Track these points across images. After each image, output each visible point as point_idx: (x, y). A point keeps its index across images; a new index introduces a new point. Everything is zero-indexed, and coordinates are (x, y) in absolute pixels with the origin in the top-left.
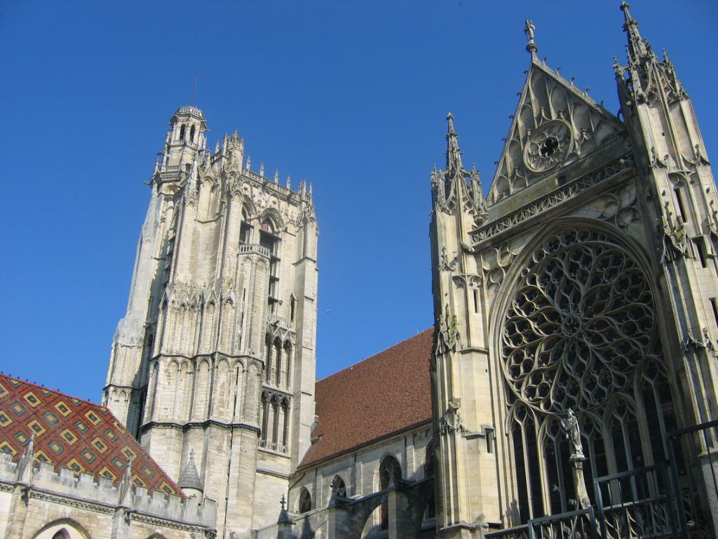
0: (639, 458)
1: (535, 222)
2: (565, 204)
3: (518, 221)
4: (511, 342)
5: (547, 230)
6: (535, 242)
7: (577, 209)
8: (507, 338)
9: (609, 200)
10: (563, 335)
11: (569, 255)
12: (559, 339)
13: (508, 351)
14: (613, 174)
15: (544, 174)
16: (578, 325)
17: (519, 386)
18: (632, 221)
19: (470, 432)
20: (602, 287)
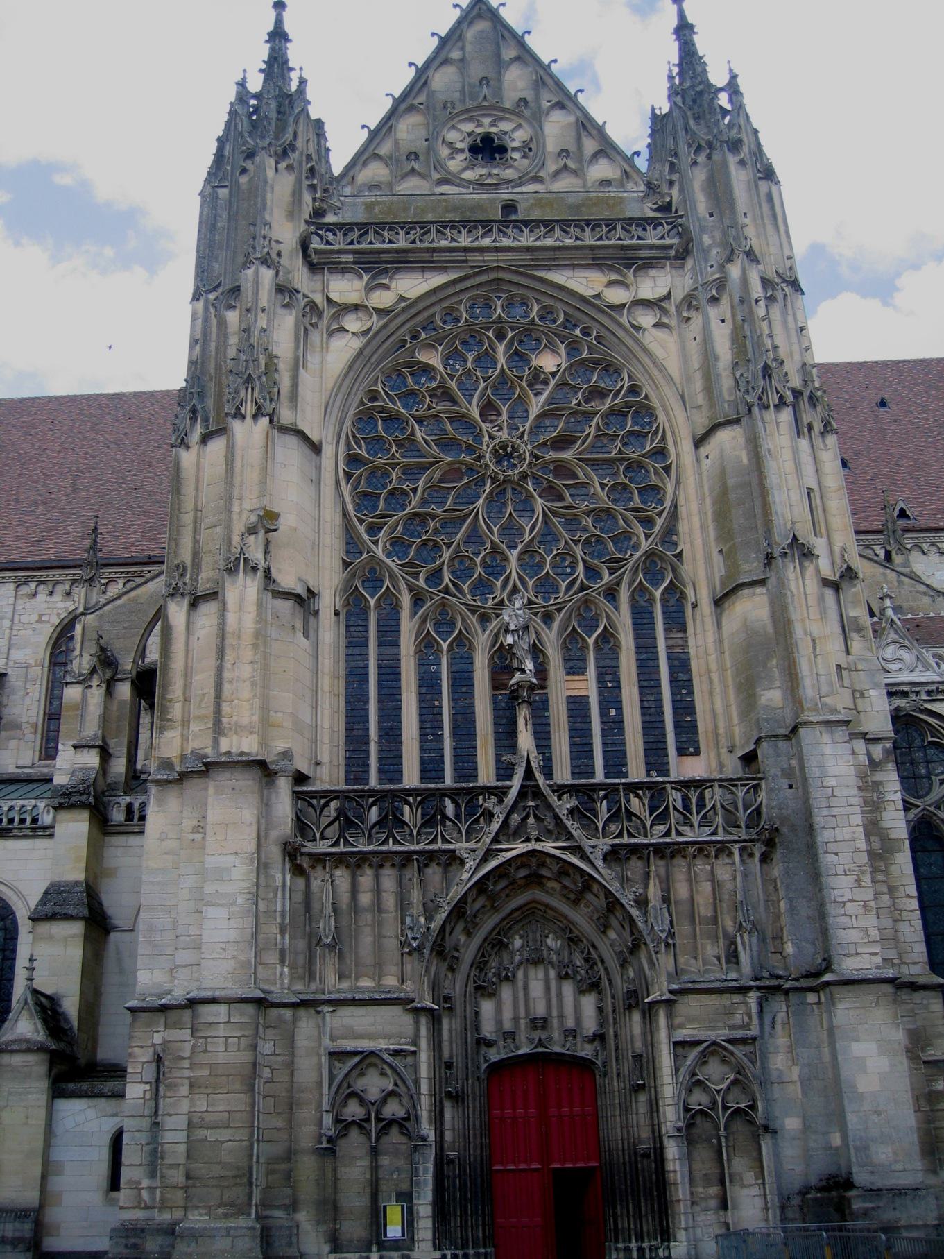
0: (613, 712)
1: (460, 256)
2: (528, 249)
3: (421, 241)
4: (364, 448)
5: (479, 280)
6: (450, 291)
7: (549, 268)
8: (354, 437)
9: (614, 277)
10: (487, 465)
11: (513, 338)
12: (470, 469)
13: (353, 460)
14: (632, 238)
15: (477, 183)
16: (521, 458)
17: (373, 529)
18: (656, 325)
19: (279, 584)
20: (574, 413)
